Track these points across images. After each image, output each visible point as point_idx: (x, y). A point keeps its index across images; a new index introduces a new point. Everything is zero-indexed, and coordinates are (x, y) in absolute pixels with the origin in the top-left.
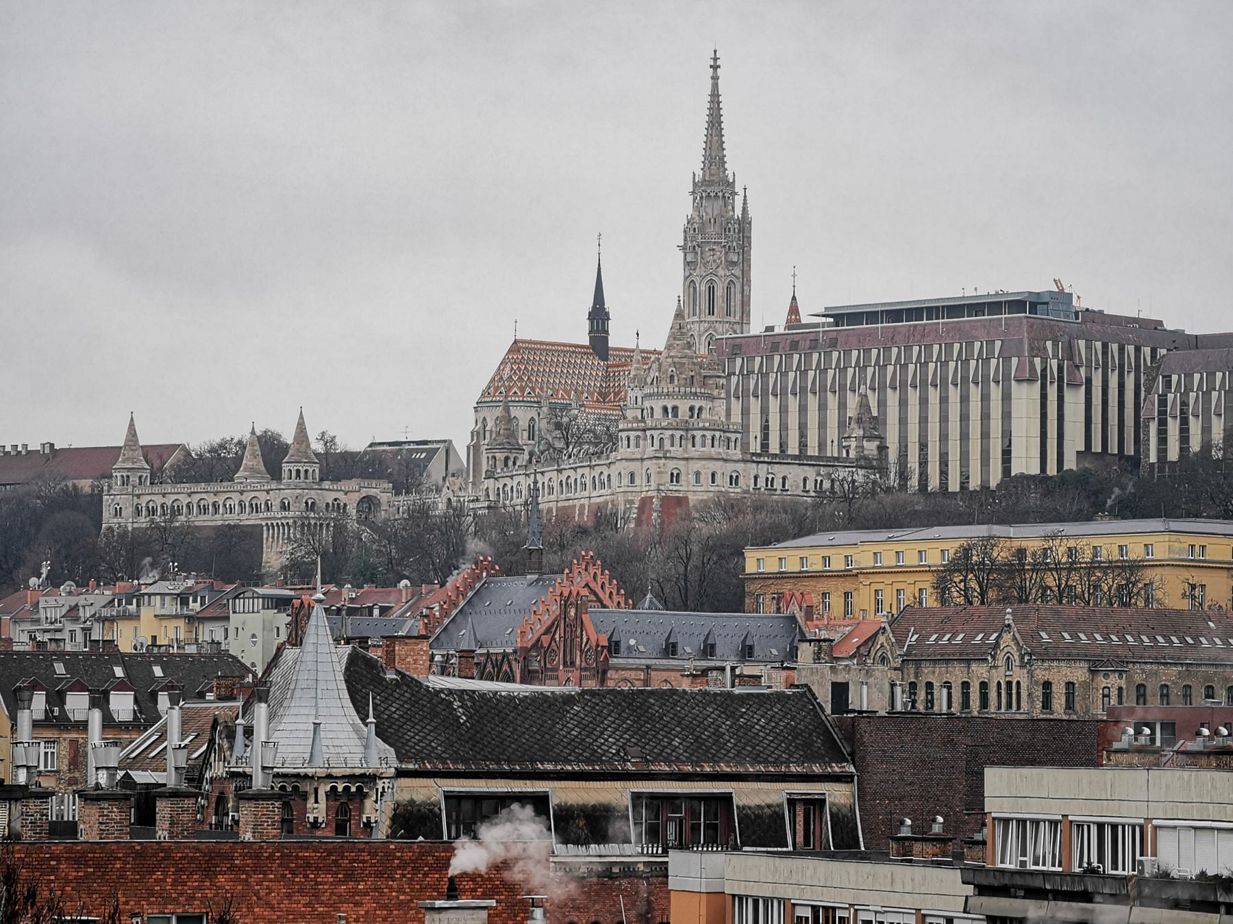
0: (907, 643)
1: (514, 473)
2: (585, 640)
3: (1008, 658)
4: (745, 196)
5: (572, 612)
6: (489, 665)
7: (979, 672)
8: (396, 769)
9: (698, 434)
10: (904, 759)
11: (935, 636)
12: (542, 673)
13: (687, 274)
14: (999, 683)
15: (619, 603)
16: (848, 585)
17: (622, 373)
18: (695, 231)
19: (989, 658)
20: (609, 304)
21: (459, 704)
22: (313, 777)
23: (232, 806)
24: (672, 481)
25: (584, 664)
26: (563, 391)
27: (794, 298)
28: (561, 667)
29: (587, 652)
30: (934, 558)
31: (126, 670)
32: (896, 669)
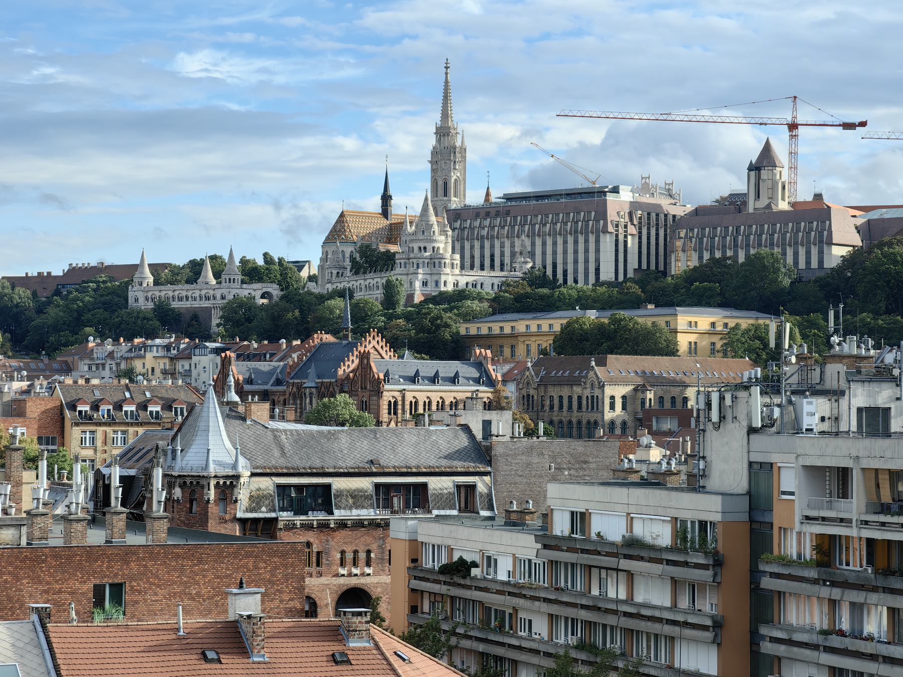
1: (342, 280)
2: (372, 375)
5: (365, 361)
7: (577, 390)
8: (251, 472)
9: (437, 261)
10: (517, 464)
11: (554, 372)
14: (587, 397)
15: (390, 356)
16: (512, 341)
20: (392, 191)
21: (285, 437)
22: (207, 477)
24: (423, 286)
27: (488, 188)
28: (360, 390)
30: (557, 328)
32: (534, 389)
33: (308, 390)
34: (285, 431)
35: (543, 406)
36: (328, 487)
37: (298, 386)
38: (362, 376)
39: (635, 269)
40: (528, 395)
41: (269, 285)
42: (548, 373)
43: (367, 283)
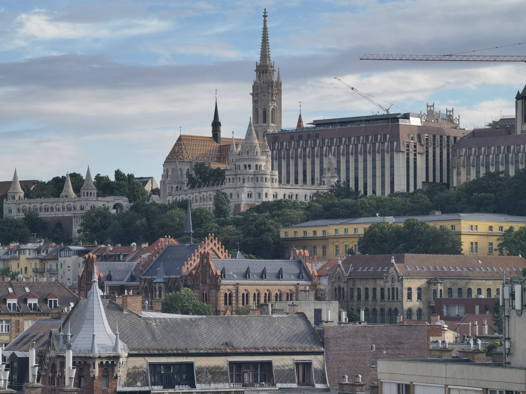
0: (349, 271)
1: (180, 193)
2: (211, 272)
3: (393, 278)
4: (279, 72)
5: (205, 261)
6: (169, 283)
7: (380, 283)
8: (128, 353)
9: (259, 177)
11: (361, 268)
12: (192, 287)
13: (254, 105)
14: (389, 288)
15: (225, 256)
17: (226, 149)
18: (257, 87)
19: (385, 278)
20: (221, 119)
21: (155, 324)
23: (58, 370)
24: (248, 197)
25: (210, 283)
26: (201, 157)
28: (201, 284)
29: (212, 278)
30: (361, 232)
31: (13, 290)
32: (344, 282)
33: (157, 285)
34: (155, 319)
35: (352, 297)
36: (191, 365)
37: (149, 281)
38: (202, 273)
39: (423, 182)
40: (340, 288)
41: (120, 197)
42: (356, 269)
43: (201, 195)
